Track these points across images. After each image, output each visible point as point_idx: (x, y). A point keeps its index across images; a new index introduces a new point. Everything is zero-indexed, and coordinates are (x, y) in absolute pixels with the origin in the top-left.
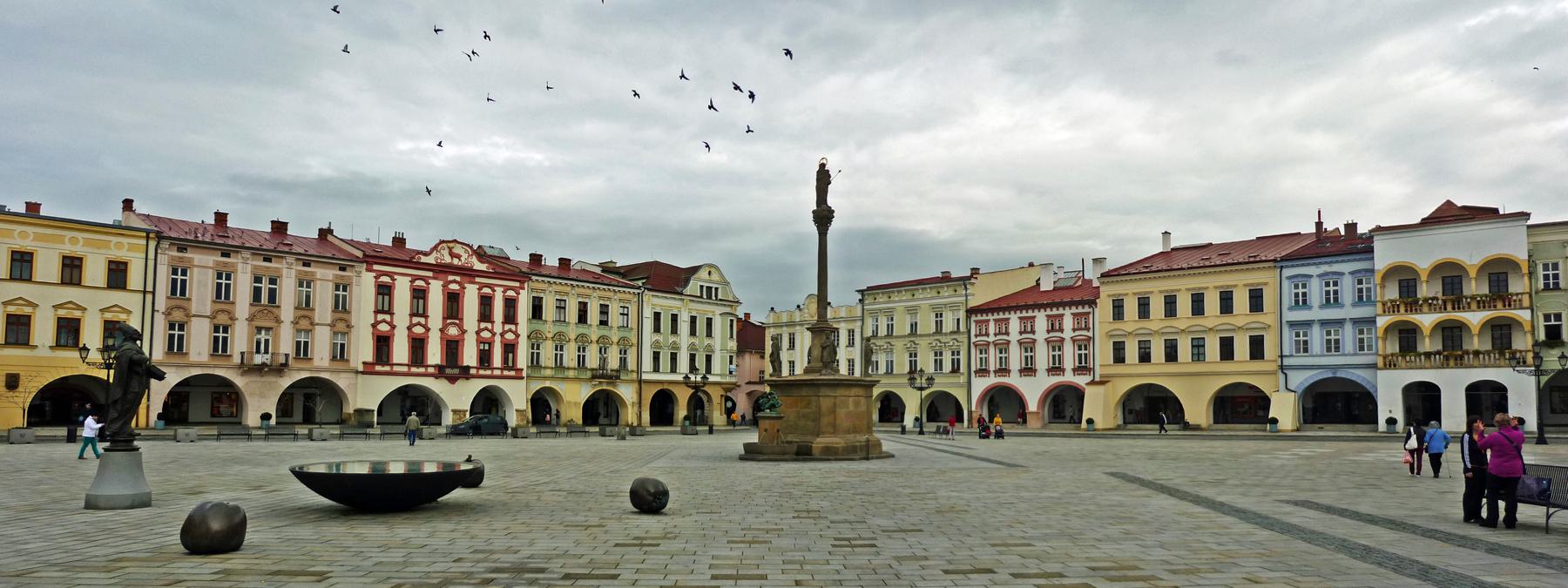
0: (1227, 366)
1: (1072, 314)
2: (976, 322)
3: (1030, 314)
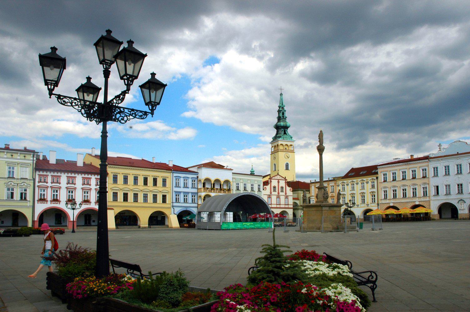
0: (155, 205)
1: (95, 178)
2: (39, 175)
3: (73, 175)
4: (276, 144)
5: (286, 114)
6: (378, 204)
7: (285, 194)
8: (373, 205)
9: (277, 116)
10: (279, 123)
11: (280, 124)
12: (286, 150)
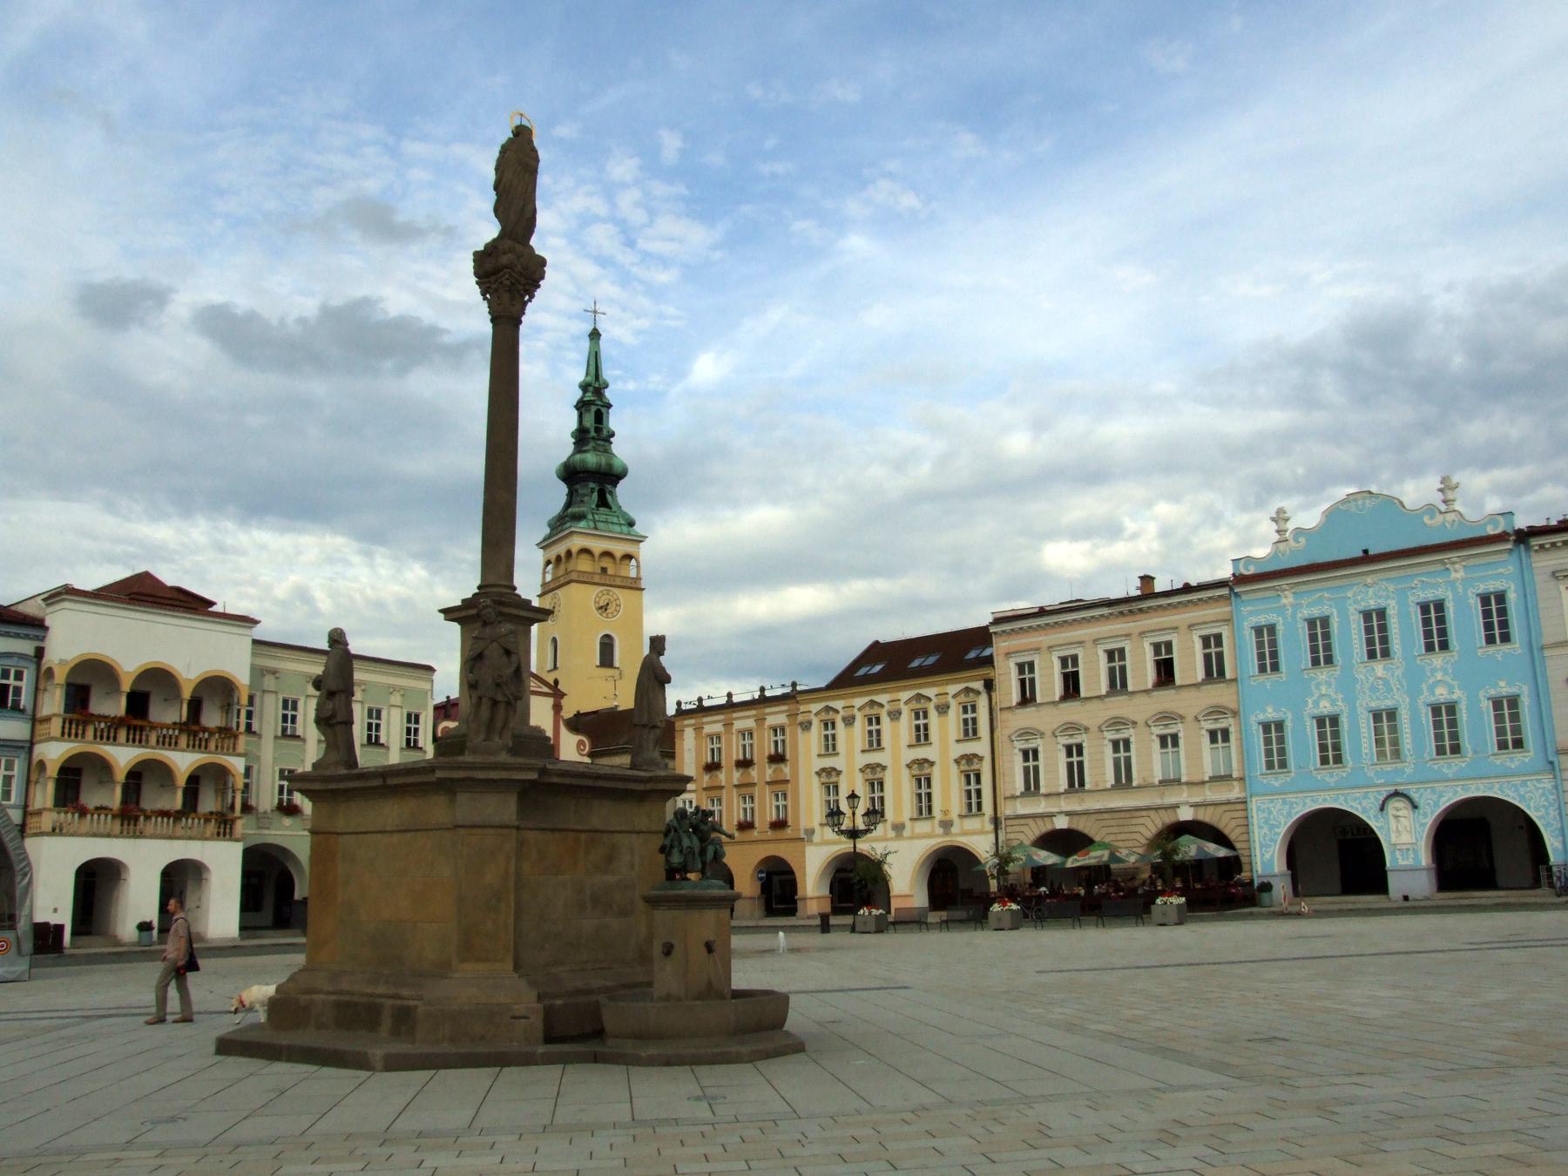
4: (561, 549)
5: (614, 421)
6: (996, 821)
8: (972, 824)
9: (573, 424)
10: (578, 457)
11: (583, 461)
12: (603, 578)
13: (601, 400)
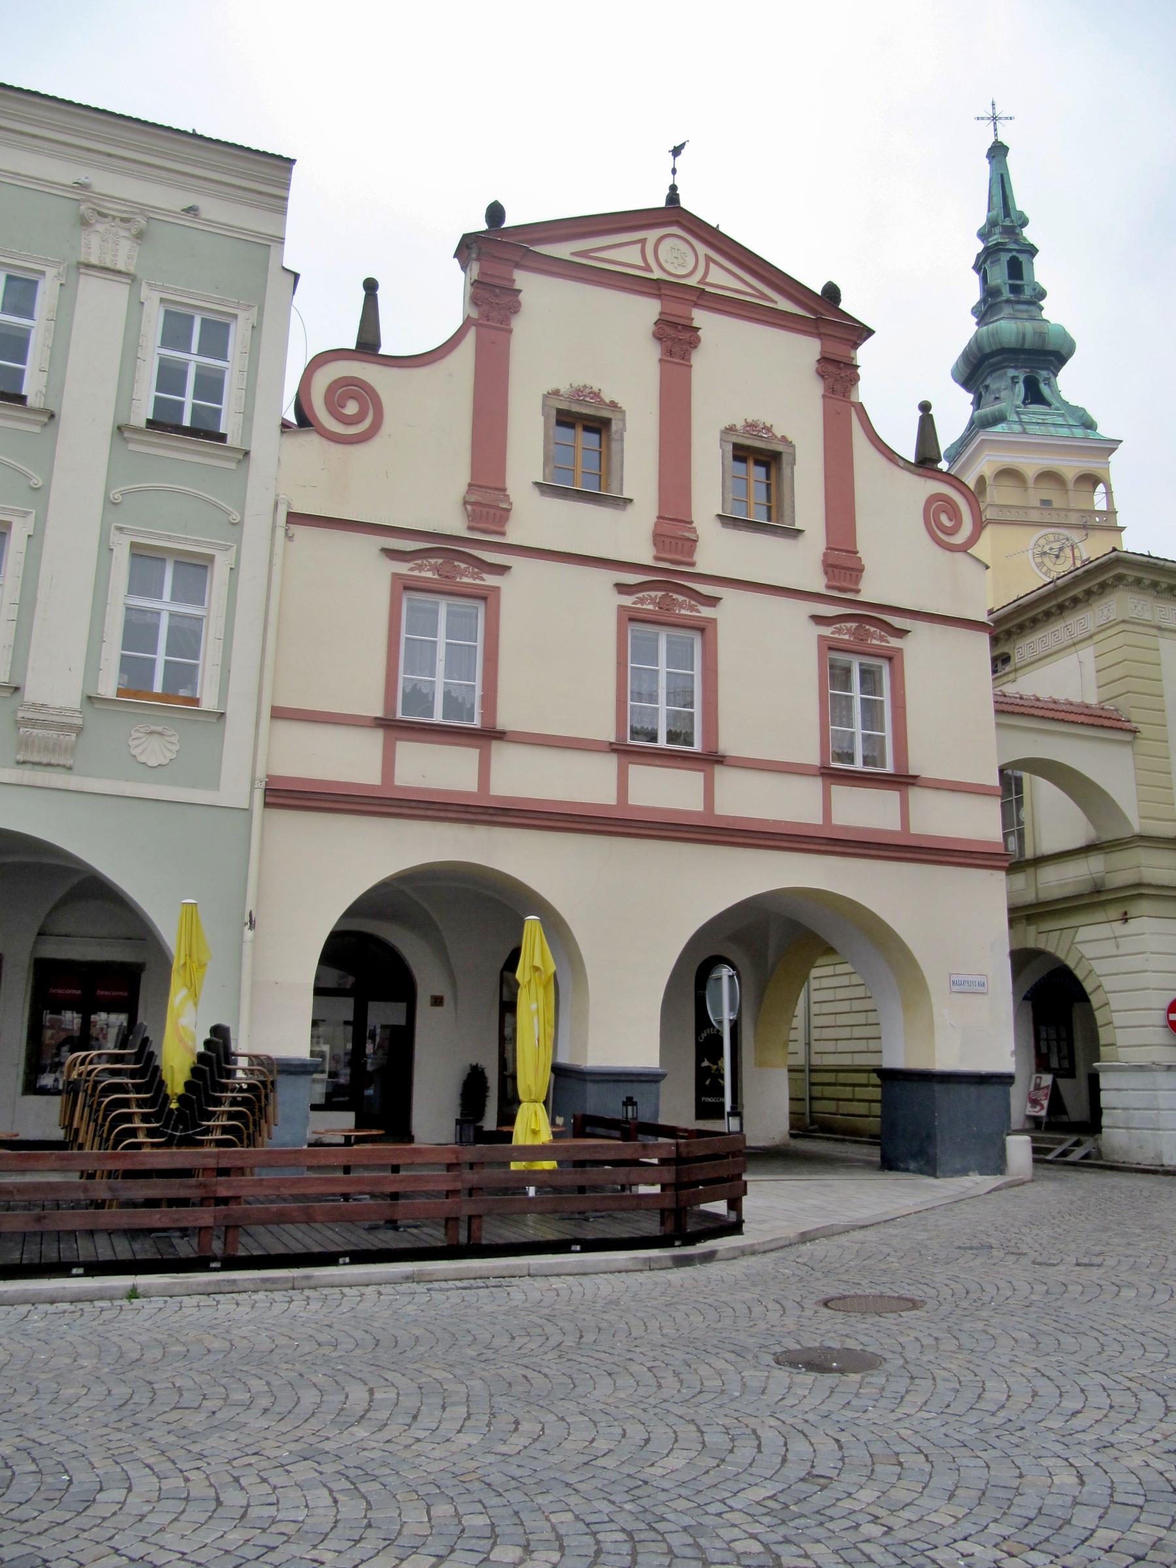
5: (1042, 271)
7: (817, 582)
11: (994, 335)
13: (1016, 242)
